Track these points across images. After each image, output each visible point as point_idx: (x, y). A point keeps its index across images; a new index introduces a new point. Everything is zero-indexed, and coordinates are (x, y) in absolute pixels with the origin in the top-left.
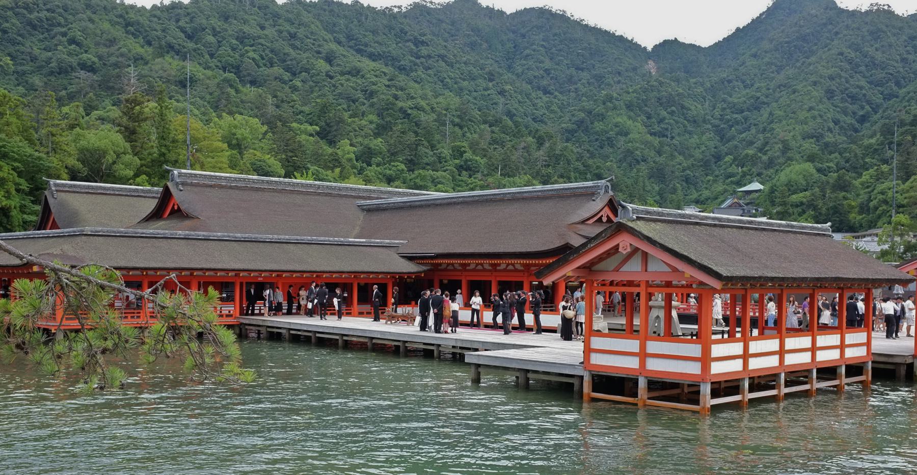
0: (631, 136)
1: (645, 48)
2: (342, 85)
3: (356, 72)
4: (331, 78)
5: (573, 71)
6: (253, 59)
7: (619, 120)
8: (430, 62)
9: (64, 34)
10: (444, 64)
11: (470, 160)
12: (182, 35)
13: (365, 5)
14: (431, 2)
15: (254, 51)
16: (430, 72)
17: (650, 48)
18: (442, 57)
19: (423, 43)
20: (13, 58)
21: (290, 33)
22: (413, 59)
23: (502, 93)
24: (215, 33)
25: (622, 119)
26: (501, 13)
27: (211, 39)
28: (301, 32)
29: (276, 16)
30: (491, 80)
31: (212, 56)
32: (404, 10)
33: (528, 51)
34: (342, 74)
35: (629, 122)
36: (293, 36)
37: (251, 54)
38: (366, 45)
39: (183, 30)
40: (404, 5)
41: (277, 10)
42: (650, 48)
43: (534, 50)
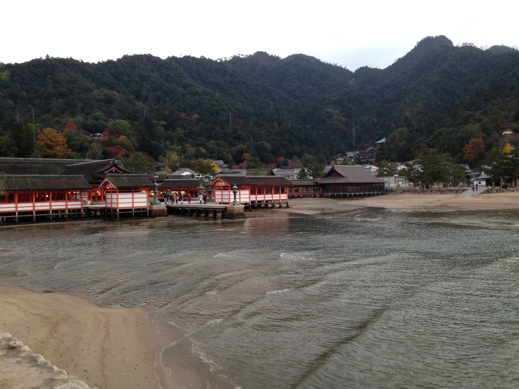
2: (189, 100)
3: (195, 93)
4: (184, 96)
5: (311, 87)
6: (147, 88)
7: (329, 110)
9: (51, 79)
11: (240, 135)
14: (242, 55)
15: (147, 84)
17: (354, 71)
20: (27, 91)
21: (165, 74)
22: (229, 85)
23: (273, 99)
24: (128, 75)
26: (278, 58)
27: (126, 78)
30: (268, 93)
31: (126, 87)
33: (288, 78)
34: (189, 94)
35: (333, 111)
36: (168, 76)
37: (146, 86)
39: (112, 74)
42: (354, 71)
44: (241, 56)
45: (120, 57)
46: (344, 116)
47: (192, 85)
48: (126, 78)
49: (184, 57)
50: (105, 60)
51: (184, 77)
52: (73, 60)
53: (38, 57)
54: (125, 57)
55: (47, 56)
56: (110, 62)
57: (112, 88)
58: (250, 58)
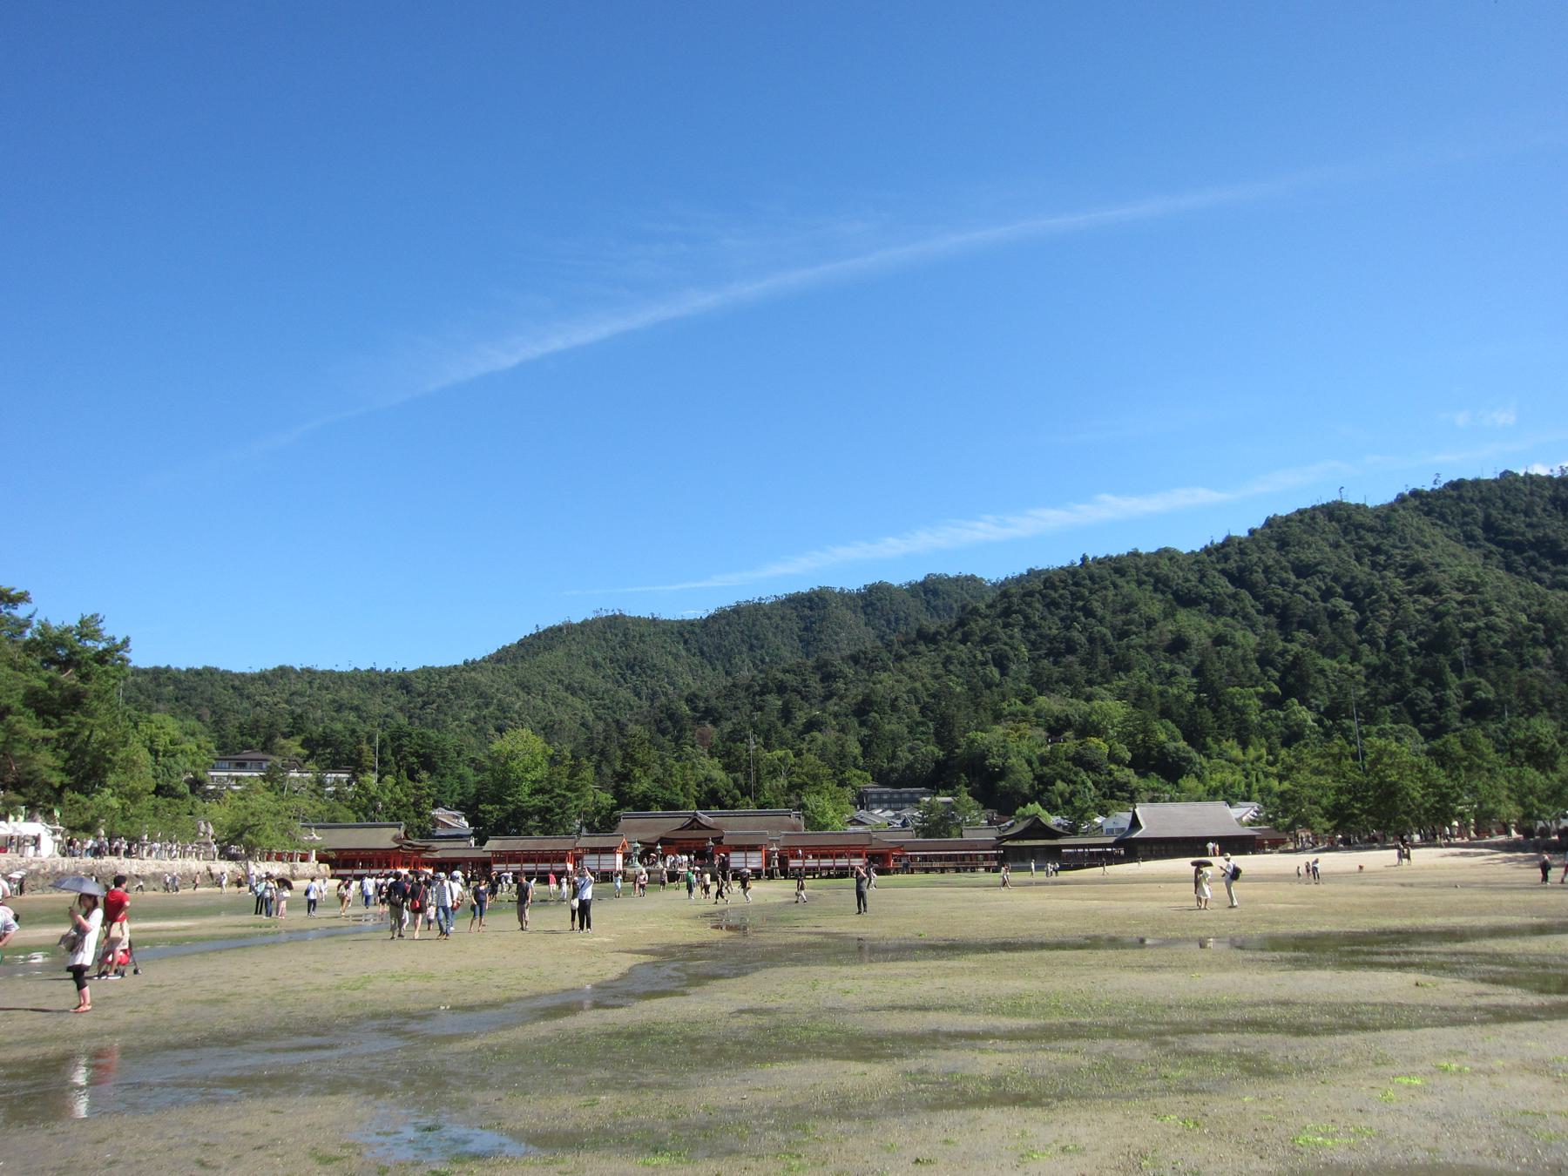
3: (1430, 589)
6: (1306, 594)
12: (1224, 581)
24: (1266, 570)
28: (1386, 544)
29: (1359, 526)
34: (1410, 593)
36: (1376, 550)
37: (1303, 588)
38: (1510, 532)
45: (1258, 523)
47: (1437, 565)
48: (1259, 577)
50: (1219, 540)
51: (1426, 546)
53: (1066, 564)
54: (1269, 523)
55: (1084, 559)
56: (1229, 541)
57: (1217, 609)
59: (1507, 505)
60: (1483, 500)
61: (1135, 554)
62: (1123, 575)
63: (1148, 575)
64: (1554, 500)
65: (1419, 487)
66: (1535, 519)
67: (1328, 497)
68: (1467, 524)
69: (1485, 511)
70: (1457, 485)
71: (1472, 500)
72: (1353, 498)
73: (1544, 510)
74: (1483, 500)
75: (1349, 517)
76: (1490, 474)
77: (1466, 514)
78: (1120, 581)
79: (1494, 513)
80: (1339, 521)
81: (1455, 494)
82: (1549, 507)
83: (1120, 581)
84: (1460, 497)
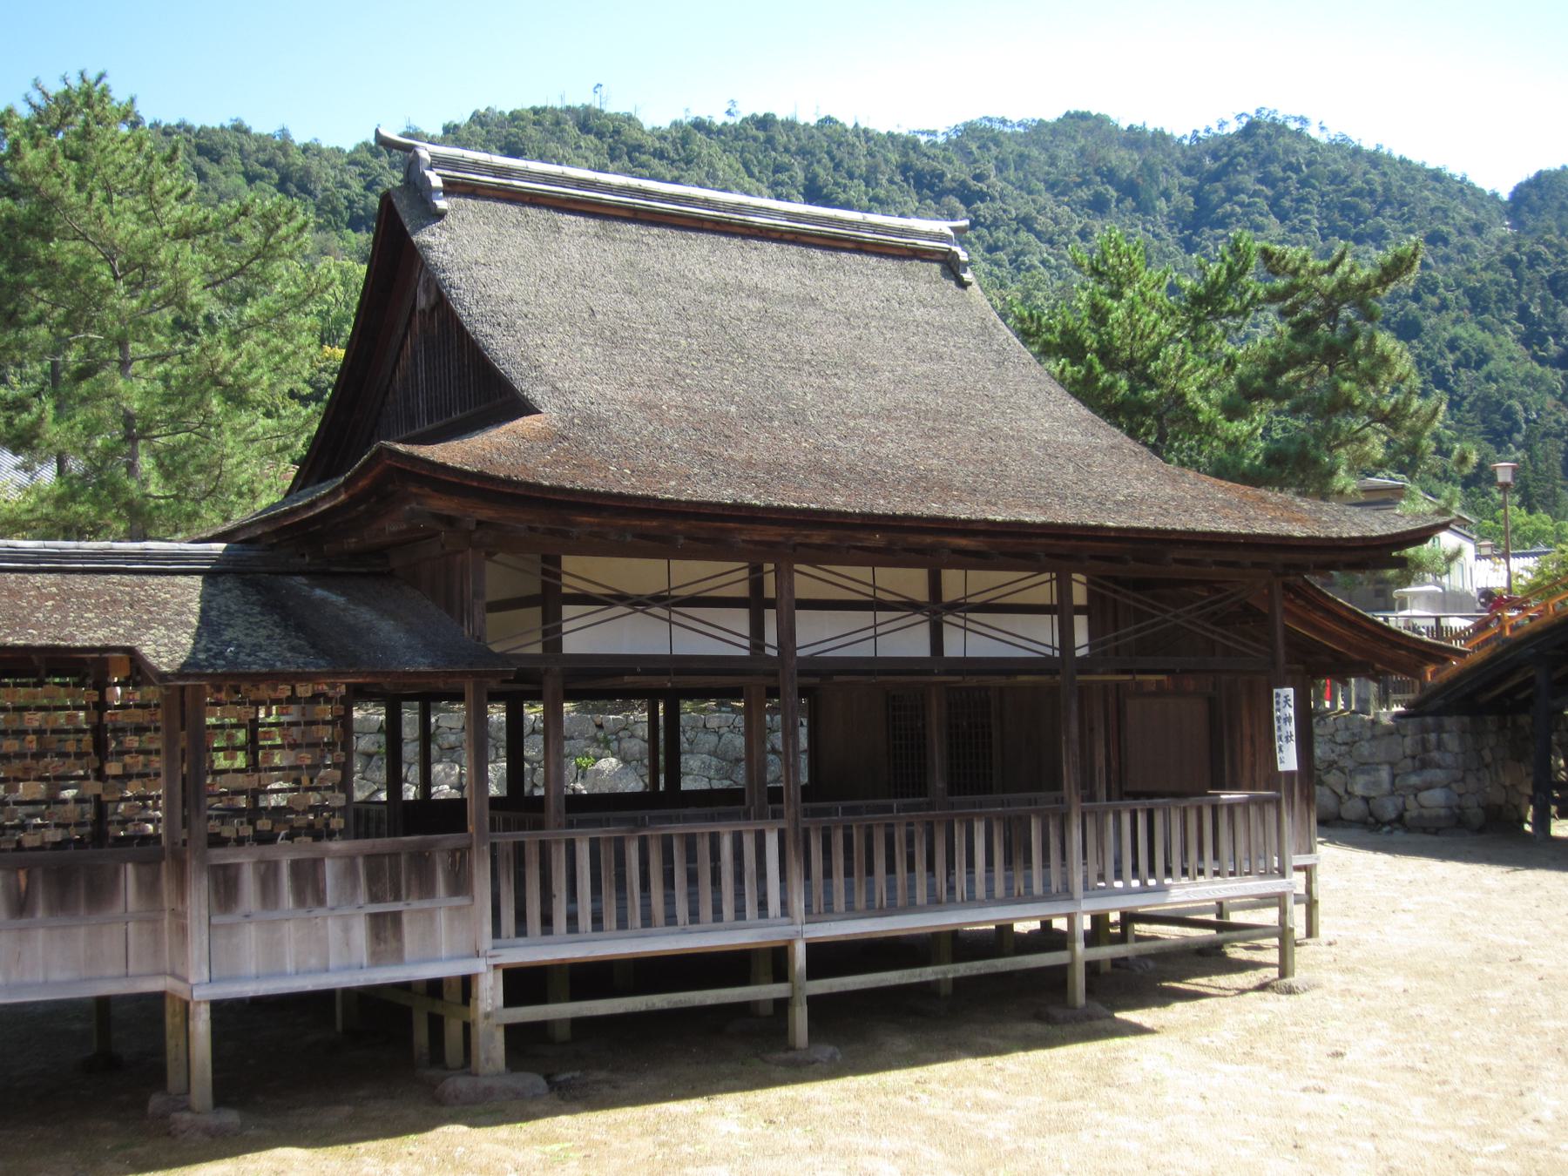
0: (1490, 367)
1: (1494, 196)
7: (1459, 330)
8: (1001, 234)
10: (1032, 237)
13: (850, 126)
14: (1003, 122)
16: (1001, 255)
17: (1505, 195)
18: (1026, 222)
19: (982, 196)
25: (1470, 332)
32: (941, 139)
40: (941, 131)
41: (637, 135)
43: (1241, 205)
44: (997, 126)
46: (1542, 361)
49: (745, 120)
52: (247, 132)
58: (1040, 133)
59: (837, 167)
60: (803, 152)
61: (239, 129)
62: (216, 158)
63: (268, 164)
64: (905, 169)
65: (704, 116)
66: (882, 193)
67: (579, 98)
68: (782, 184)
69: (806, 169)
70: (765, 123)
71: (787, 150)
72: (614, 105)
73: (891, 181)
74: (803, 152)
75: (617, 132)
76: (808, 116)
77: (778, 169)
78: (211, 169)
79: (822, 173)
80: (600, 135)
81: (761, 135)
82: (898, 178)
83: (211, 169)
84: (770, 140)
